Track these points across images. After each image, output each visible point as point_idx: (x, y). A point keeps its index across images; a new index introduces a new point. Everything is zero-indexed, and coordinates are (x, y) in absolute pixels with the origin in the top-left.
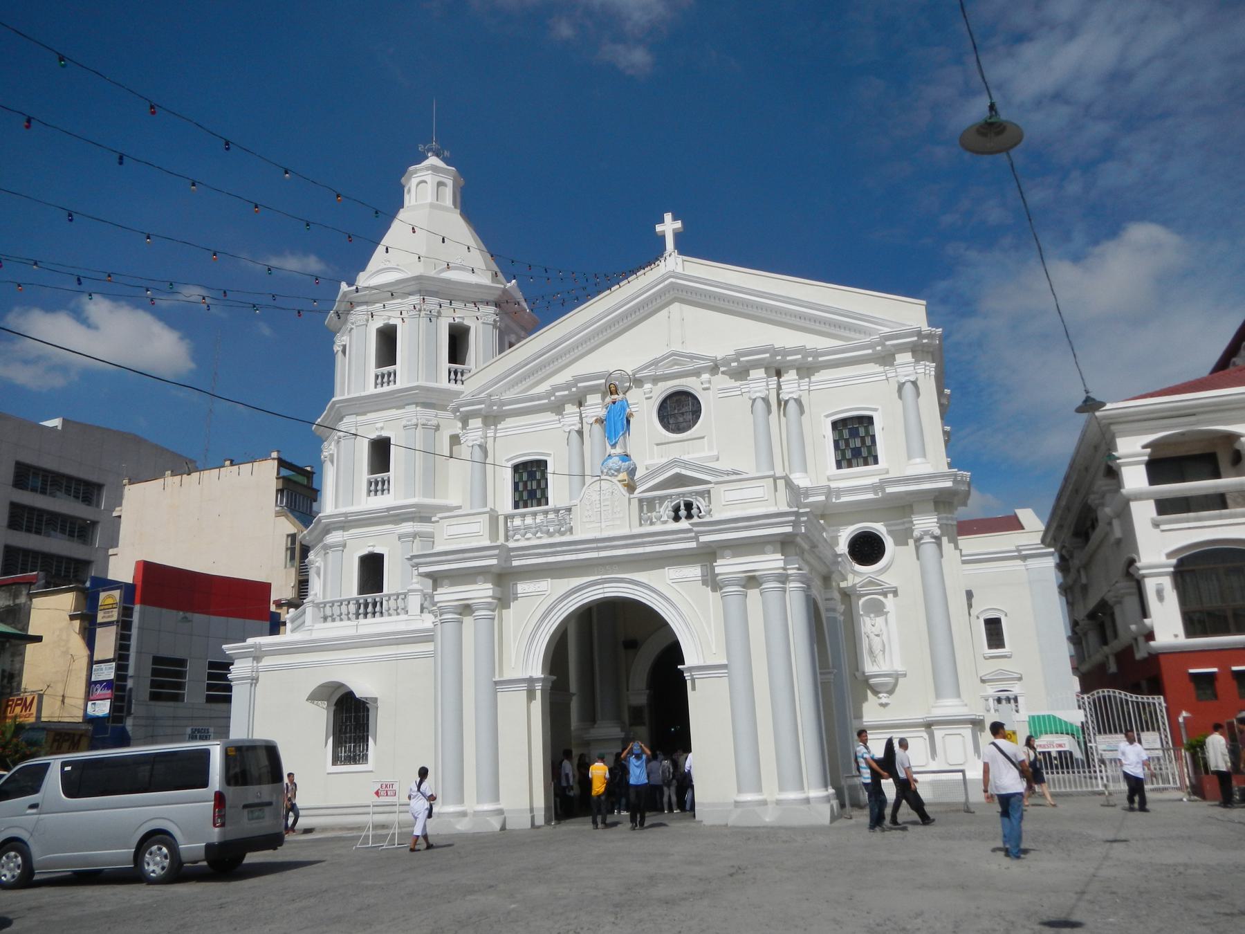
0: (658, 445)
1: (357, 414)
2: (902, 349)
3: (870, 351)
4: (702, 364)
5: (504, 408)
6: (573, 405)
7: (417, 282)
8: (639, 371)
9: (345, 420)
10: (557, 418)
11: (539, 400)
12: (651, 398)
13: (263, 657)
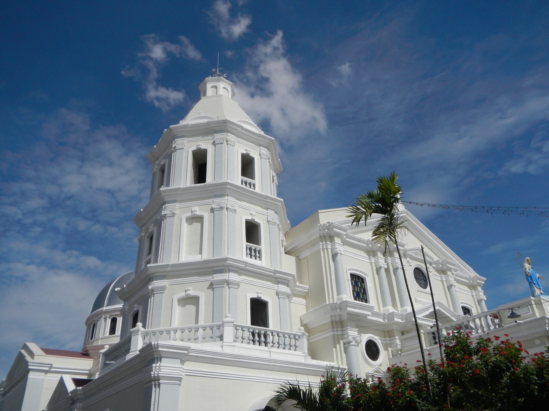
0: (418, 291)
1: (237, 199)
2: (479, 284)
3: (468, 281)
5: (347, 239)
6: (381, 253)
8: (408, 251)
9: (226, 198)
10: (367, 256)
12: (411, 266)
13: (185, 361)
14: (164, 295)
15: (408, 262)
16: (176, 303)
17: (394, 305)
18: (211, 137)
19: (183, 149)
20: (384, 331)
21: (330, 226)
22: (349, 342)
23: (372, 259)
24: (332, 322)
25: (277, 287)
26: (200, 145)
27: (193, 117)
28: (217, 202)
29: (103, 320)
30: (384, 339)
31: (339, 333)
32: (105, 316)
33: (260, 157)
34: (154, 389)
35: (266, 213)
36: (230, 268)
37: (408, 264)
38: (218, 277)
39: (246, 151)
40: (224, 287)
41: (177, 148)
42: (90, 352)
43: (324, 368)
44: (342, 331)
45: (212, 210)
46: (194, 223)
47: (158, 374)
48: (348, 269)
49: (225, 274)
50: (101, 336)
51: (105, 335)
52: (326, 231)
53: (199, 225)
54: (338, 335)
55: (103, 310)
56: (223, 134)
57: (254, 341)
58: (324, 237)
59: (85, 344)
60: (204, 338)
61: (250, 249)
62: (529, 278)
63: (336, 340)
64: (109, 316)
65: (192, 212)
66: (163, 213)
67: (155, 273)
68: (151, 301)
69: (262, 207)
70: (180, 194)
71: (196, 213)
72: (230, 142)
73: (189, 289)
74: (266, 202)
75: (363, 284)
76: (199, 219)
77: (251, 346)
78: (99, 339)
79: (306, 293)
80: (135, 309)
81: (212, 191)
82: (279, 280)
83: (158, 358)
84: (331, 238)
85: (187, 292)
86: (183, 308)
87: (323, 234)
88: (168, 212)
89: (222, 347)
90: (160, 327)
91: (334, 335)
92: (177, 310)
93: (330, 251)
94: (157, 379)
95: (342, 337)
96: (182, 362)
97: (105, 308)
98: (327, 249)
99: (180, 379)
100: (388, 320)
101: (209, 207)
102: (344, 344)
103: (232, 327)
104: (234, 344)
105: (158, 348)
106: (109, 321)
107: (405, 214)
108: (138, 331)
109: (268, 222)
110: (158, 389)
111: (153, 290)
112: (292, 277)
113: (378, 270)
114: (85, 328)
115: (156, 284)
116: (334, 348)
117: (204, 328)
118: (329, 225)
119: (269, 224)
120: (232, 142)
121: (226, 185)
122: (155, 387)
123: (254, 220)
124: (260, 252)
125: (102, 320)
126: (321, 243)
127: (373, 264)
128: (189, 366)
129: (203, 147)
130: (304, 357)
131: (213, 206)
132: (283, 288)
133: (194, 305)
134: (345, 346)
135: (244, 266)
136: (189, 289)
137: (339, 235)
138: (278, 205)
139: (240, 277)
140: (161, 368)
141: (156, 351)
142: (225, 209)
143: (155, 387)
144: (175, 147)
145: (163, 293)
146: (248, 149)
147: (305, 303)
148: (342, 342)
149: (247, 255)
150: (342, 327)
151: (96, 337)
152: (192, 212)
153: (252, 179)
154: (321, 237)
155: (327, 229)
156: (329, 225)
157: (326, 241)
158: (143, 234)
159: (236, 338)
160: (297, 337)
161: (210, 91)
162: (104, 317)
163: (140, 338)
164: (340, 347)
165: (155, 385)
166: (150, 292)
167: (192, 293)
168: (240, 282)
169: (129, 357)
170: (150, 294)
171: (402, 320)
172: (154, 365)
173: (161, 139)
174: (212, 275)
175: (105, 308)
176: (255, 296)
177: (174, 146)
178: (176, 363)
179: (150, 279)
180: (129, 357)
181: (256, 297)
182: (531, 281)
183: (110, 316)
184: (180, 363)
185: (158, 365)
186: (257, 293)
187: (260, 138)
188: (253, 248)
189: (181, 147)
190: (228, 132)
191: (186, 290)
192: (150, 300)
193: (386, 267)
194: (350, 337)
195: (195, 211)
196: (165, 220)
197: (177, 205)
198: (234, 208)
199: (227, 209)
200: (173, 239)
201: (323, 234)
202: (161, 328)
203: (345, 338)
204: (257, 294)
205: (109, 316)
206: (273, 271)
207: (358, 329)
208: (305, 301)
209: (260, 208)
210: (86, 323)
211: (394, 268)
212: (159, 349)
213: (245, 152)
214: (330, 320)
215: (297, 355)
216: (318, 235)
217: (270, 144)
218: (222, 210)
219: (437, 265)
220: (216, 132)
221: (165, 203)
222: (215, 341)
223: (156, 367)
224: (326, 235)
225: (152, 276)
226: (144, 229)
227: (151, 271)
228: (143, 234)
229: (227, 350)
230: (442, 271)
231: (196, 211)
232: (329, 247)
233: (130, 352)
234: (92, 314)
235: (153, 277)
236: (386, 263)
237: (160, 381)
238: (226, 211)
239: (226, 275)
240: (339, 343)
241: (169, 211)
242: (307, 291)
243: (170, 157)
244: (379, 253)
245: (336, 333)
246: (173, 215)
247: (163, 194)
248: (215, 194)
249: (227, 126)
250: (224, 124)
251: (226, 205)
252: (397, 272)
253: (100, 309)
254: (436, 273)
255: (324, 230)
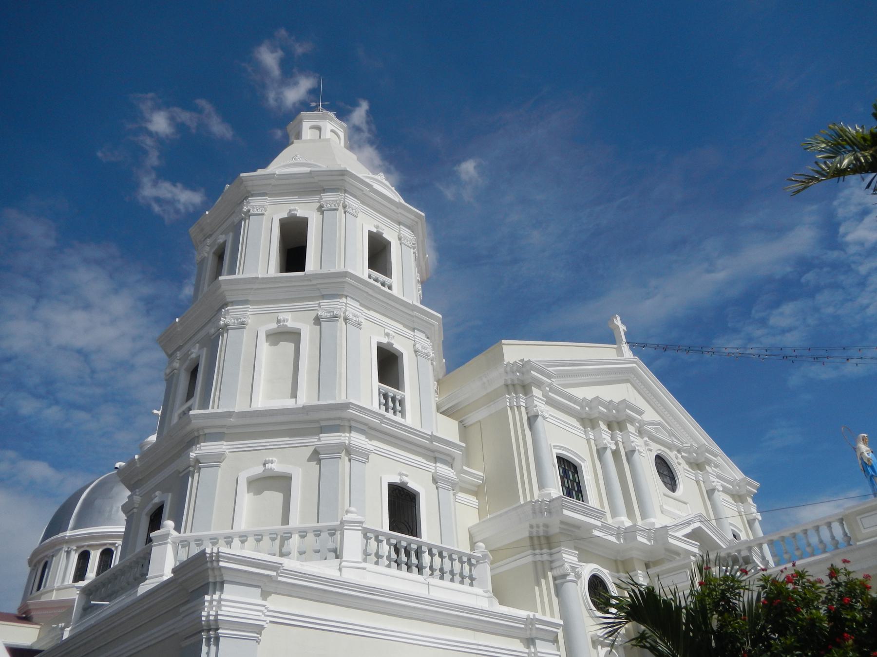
1: (361, 305)
4: (676, 442)
7: (417, 219)
8: (647, 424)
9: (344, 300)
10: (581, 427)
11: (574, 403)
14: (220, 470)
15: (645, 443)
16: (243, 486)
17: (630, 514)
18: (316, 198)
19: (263, 214)
20: (616, 561)
21: (524, 366)
22: (565, 576)
23: (590, 433)
24: (531, 538)
25: (434, 468)
26: (294, 210)
27: (282, 164)
28: (326, 307)
29: (63, 555)
30: (616, 574)
31: (546, 557)
32: (68, 548)
33: (399, 242)
34: (204, 649)
35: (413, 336)
36: (353, 424)
37: (647, 448)
38: (328, 439)
39: (377, 228)
40: (340, 458)
41: (252, 212)
42: (33, 613)
43: (524, 621)
44: (551, 554)
45: (318, 321)
46: (281, 343)
47: (216, 615)
48: (553, 446)
49: (343, 435)
50: (57, 584)
51: (66, 583)
52: (518, 374)
53: (290, 346)
54: (542, 562)
55: (66, 536)
56: (339, 195)
57: (398, 563)
58: (514, 385)
59: (25, 598)
60: (302, 553)
61: (385, 396)
62: (869, 469)
63: (540, 570)
64: (75, 548)
65: (278, 321)
66: (222, 323)
67: (203, 428)
68: (193, 482)
69: (405, 326)
70: (256, 289)
71: (285, 323)
72: (351, 209)
73: (272, 460)
74: (412, 316)
75: (576, 476)
76: (294, 336)
77: (394, 571)
78: (52, 591)
79: (479, 486)
80: (156, 500)
81: (318, 286)
82: (437, 455)
83: (215, 583)
84: (525, 388)
85: (267, 465)
86: (259, 496)
87: (512, 380)
88: (233, 321)
89: (340, 570)
90: (210, 531)
91: (535, 563)
92: (246, 499)
93: (523, 410)
94: (214, 627)
95: (550, 565)
96: (265, 595)
97: (68, 533)
98: (519, 407)
99: (259, 629)
100: (625, 539)
101: (313, 315)
102: (555, 579)
103: (360, 532)
104: (363, 565)
105: (218, 561)
106: (75, 557)
107: (634, 365)
108: (167, 536)
109: (416, 351)
110: (213, 648)
111: (197, 461)
112: (461, 451)
113: (601, 452)
114: (27, 569)
115: (205, 448)
116: (537, 586)
117: (303, 534)
118: (523, 365)
119: (416, 356)
120: (352, 210)
121: (346, 277)
122: (208, 645)
123: (393, 344)
124: (402, 402)
125: (61, 554)
126: (509, 396)
127: (592, 442)
128: (278, 603)
129: (300, 213)
130: (487, 599)
131: (319, 313)
132: (443, 470)
133: (279, 491)
134: (557, 582)
135: (379, 422)
136: (272, 460)
137: (539, 385)
138: (433, 325)
139: (370, 442)
140: (223, 603)
141: (213, 569)
142: (341, 320)
143: (208, 645)
144: (249, 211)
145: (218, 466)
146: (380, 225)
147: (477, 504)
148: (550, 574)
149: (380, 405)
150: (550, 548)
151: (47, 586)
152: (278, 321)
153: (386, 275)
154: (507, 386)
155: (518, 372)
156: (523, 365)
157: (516, 393)
158: (176, 365)
159: (366, 554)
160: (473, 561)
161: (307, 132)
162: (66, 549)
163: (170, 548)
164: (547, 584)
165: (208, 639)
166: (192, 463)
167: (277, 467)
168: (371, 451)
169: (144, 588)
170: (191, 469)
171: (649, 540)
172: (207, 598)
173: (220, 198)
174: (319, 435)
175: (68, 533)
176: (396, 480)
177: (245, 209)
178: (252, 596)
179: (193, 441)
180: (144, 588)
181: (399, 482)
182: (873, 474)
183: (78, 547)
184: (261, 596)
185: (216, 597)
186: (401, 474)
187: (400, 211)
188: (391, 394)
189: (260, 212)
190: (345, 191)
191: (266, 461)
192: (190, 479)
193: (614, 447)
194: (567, 566)
195: (284, 321)
196: (225, 335)
197: (251, 309)
198: (358, 319)
199: (346, 319)
200: (241, 369)
201: (512, 380)
202: (213, 532)
203: (556, 568)
204: (399, 477)
205: (75, 548)
206: (429, 437)
207: (578, 553)
208: (477, 501)
209: (402, 326)
210: (30, 562)
211: (626, 451)
212: (221, 564)
213: (375, 230)
214: (527, 534)
215: (476, 595)
216: (502, 382)
217: (417, 222)
218: (337, 321)
219: (690, 453)
220: (324, 191)
221: (226, 305)
222: (326, 559)
223: (211, 602)
224: (516, 382)
225: (196, 434)
226: (178, 355)
227: (195, 424)
228: (176, 365)
229: (349, 576)
230: (697, 465)
231: (287, 320)
232: (522, 403)
233: (146, 579)
234: (43, 543)
235: (198, 437)
236: (614, 442)
237: (220, 631)
238: (344, 323)
239: (345, 437)
240: (545, 577)
241: (234, 319)
242: (481, 482)
243: (236, 229)
244: (601, 423)
245: (538, 558)
246: (242, 325)
247: (223, 287)
248: (323, 293)
249: (345, 181)
250: (340, 178)
251: (344, 313)
252: (633, 457)
253: (60, 534)
254: (687, 467)
255: (513, 372)
